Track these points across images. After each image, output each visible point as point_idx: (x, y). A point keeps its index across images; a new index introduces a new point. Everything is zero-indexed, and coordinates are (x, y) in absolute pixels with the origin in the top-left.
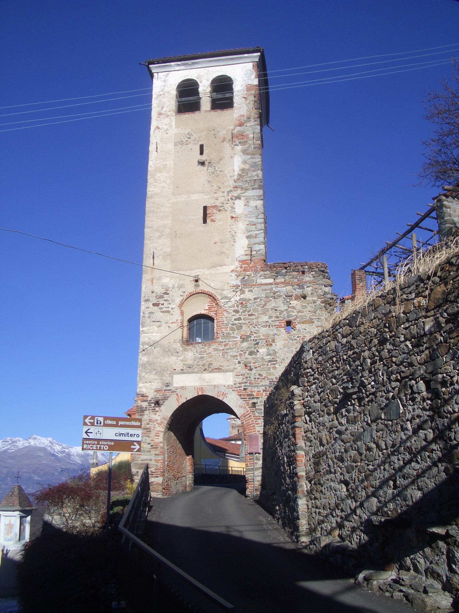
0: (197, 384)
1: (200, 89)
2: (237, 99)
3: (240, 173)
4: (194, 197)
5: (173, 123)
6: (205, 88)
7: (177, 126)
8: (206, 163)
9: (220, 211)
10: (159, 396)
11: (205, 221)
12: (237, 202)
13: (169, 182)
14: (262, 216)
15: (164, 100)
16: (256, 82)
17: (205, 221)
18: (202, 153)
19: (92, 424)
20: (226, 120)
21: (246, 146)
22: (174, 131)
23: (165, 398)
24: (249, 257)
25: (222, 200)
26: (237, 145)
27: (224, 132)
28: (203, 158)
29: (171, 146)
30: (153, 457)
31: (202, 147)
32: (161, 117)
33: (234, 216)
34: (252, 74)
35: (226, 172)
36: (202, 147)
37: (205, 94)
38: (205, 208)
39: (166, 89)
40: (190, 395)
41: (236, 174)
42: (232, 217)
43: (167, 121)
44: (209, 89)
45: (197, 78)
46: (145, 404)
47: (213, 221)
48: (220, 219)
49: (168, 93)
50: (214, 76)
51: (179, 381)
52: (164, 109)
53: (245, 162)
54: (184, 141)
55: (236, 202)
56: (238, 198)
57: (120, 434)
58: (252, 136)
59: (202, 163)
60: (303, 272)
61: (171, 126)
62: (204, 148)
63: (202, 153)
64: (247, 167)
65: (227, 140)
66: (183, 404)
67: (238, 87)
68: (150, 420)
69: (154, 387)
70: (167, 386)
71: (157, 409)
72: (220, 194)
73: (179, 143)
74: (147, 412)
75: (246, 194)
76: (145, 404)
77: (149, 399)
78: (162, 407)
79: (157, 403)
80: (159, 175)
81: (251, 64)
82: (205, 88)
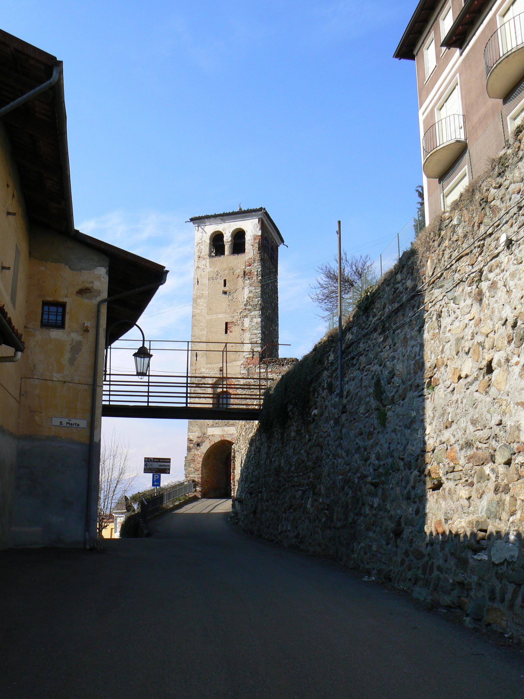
0: (221, 433)
1: (225, 239)
2: (248, 246)
3: (248, 299)
4: (220, 316)
5: (208, 264)
6: (227, 238)
7: (210, 267)
8: (228, 293)
9: (235, 325)
10: (199, 441)
11: (226, 332)
12: (246, 319)
13: (205, 305)
14: (260, 329)
15: (202, 247)
16: (260, 233)
17: (226, 332)
18: (225, 285)
19: (148, 461)
20: (239, 262)
21: (253, 281)
22: (208, 269)
23: (203, 442)
24: (251, 355)
25: (236, 317)
26: (246, 280)
27: (239, 271)
28: (226, 289)
29: (206, 281)
30: (196, 476)
31: (225, 281)
32: (201, 259)
33: (243, 328)
34: (258, 227)
35: (240, 299)
36: (225, 281)
37: (228, 242)
38: (227, 324)
39: (203, 239)
40: (217, 440)
41: (245, 300)
42: (242, 330)
43: (204, 262)
44: (230, 239)
45: (223, 230)
46: (191, 445)
47: (231, 332)
48: (235, 330)
49: (205, 241)
50: (234, 229)
51: (211, 431)
52: (202, 254)
53: (250, 292)
54: (215, 277)
55: (245, 319)
56: (246, 316)
57: (161, 466)
58: (256, 273)
59: (225, 293)
60: (283, 365)
61: (206, 266)
62: (227, 282)
63: (225, 285)
64: (251, 295)
65: (240, 277)
66: (213, 445)
67: (248, 238)
68: (195, 455)
69: (196, 435)
70: (204, 435)
71: (198, 448)
72: (235, 314)
73: (211, 279)
74: (193, 450)
75: (251, 314)
76: (191, 445)
77: (194, 442)
78: (201, 447)
79: (198, 445)
80: (199, 301)
81: (257, 220)
82: (227, 238)
